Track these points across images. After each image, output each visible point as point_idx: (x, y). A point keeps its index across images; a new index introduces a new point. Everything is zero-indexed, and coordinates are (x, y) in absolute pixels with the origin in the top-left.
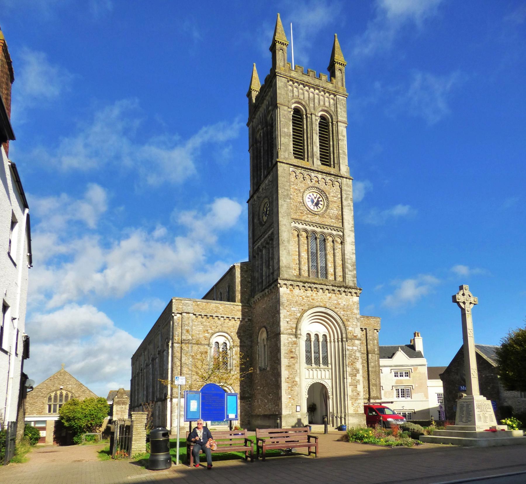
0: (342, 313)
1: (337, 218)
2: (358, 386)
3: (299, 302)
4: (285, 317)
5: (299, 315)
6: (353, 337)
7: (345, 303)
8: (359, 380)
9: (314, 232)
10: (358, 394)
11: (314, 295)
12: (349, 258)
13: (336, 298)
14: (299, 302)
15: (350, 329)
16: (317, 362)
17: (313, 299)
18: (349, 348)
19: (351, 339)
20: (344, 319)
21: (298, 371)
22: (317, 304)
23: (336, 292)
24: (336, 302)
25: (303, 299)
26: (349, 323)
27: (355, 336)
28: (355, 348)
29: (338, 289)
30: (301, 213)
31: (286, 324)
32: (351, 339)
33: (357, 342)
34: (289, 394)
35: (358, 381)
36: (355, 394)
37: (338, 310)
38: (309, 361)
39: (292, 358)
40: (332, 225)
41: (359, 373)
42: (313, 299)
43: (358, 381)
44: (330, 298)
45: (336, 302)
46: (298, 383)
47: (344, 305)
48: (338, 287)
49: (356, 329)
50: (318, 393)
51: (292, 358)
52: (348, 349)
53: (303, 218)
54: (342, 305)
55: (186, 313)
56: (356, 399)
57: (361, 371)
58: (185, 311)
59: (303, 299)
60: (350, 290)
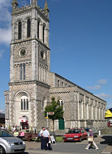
0: (29, 91)
2: (34, 117)
7: (30, 87)
8: (35, 115)
9: (21, 64)
10: (34, 120)
11: (20, 86)
12: (33, 70)
13: (27, 86)
17: (19, 88)
18: (31, 103)
19: (32, 100)
20: (30, 93)
22: (21, 89)
23: (29, 83)
24: (27, 87)
25: (16, 88)
26: (32, 94)
27: (34, 99)
28: (33, 103)
30: (18, 59)
32: (32, 100)
36: (33, 120)
37: (28, 90)
40: (28, 59)
41: (35, 112)
44: (25, 86)
45: (27, 87)
47: (30, 88)
49: (34, 96)
52: (31, 104)
54: (29, 88)
57: (36, 112)
59: (16, 88)
60: (32, 82)
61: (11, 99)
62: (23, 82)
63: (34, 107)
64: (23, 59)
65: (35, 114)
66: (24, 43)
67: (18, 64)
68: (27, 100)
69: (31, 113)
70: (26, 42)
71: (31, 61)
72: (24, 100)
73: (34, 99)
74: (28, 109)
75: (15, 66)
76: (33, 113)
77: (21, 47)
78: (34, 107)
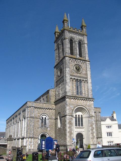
1: (85, 74)
3: (73, 104)
4: (68, 109)
5: (73, 108)
6: (92, 116)
7: (89, 104)
9: (77, 79)
14: (73, 104)
15: (91, 113)
16: (79, 125)
19: (91, 117)
21: (73, 129)
22: (79, 104)
28: (92, 120)
29: (86, 99)
31: (68, 112)
32: (91, 117)
33: (93, 118)
34: (70, 137)
35: (94, 132)
38: (76, 125)
39: (70, 124)
42: (78, 103)
43: (94, 132)
46: (73, 133)
48: (86, 98)
50: (80, 136)
51: (70, 124)
52: (90, 121)
53: (74, 75)
55: (32, 107)
56: (94, 139)
57: (95, 128)
58: (32, 106)
60: (90, 99)
61: (69, 114)
62: (84, 98)
63: (93, 124)
64: (76, 74)
65: (94, 130)
66: (79, 61)
67: (74, 79)
68: (82, 116)
69: (91, 130)
70: (81, 61)
71: (86, 80)
72: (79, 116)
73: (93, 116)
74: (82, 125)
75: (71, 80)
76: (92, 130)
77: (76, 63)
78: (93, 124)
